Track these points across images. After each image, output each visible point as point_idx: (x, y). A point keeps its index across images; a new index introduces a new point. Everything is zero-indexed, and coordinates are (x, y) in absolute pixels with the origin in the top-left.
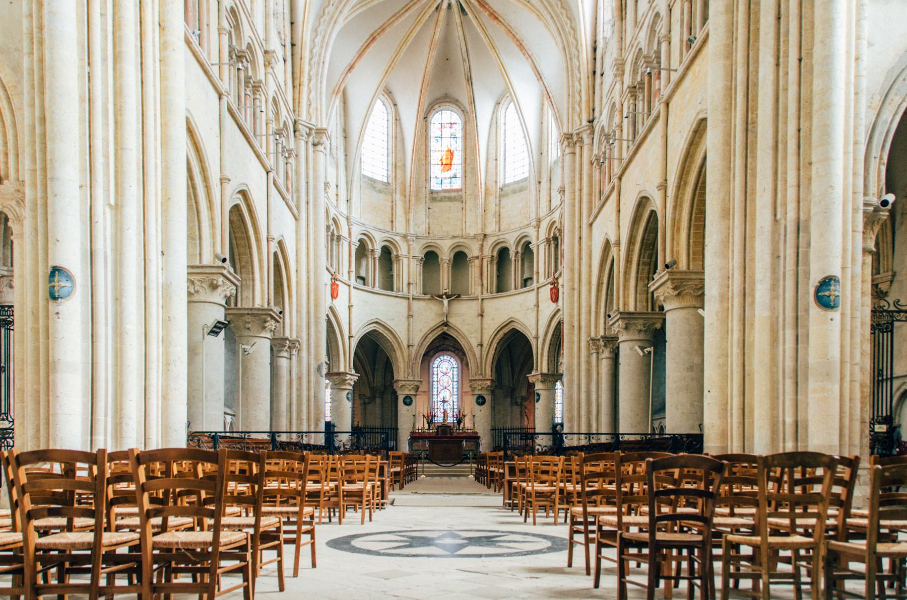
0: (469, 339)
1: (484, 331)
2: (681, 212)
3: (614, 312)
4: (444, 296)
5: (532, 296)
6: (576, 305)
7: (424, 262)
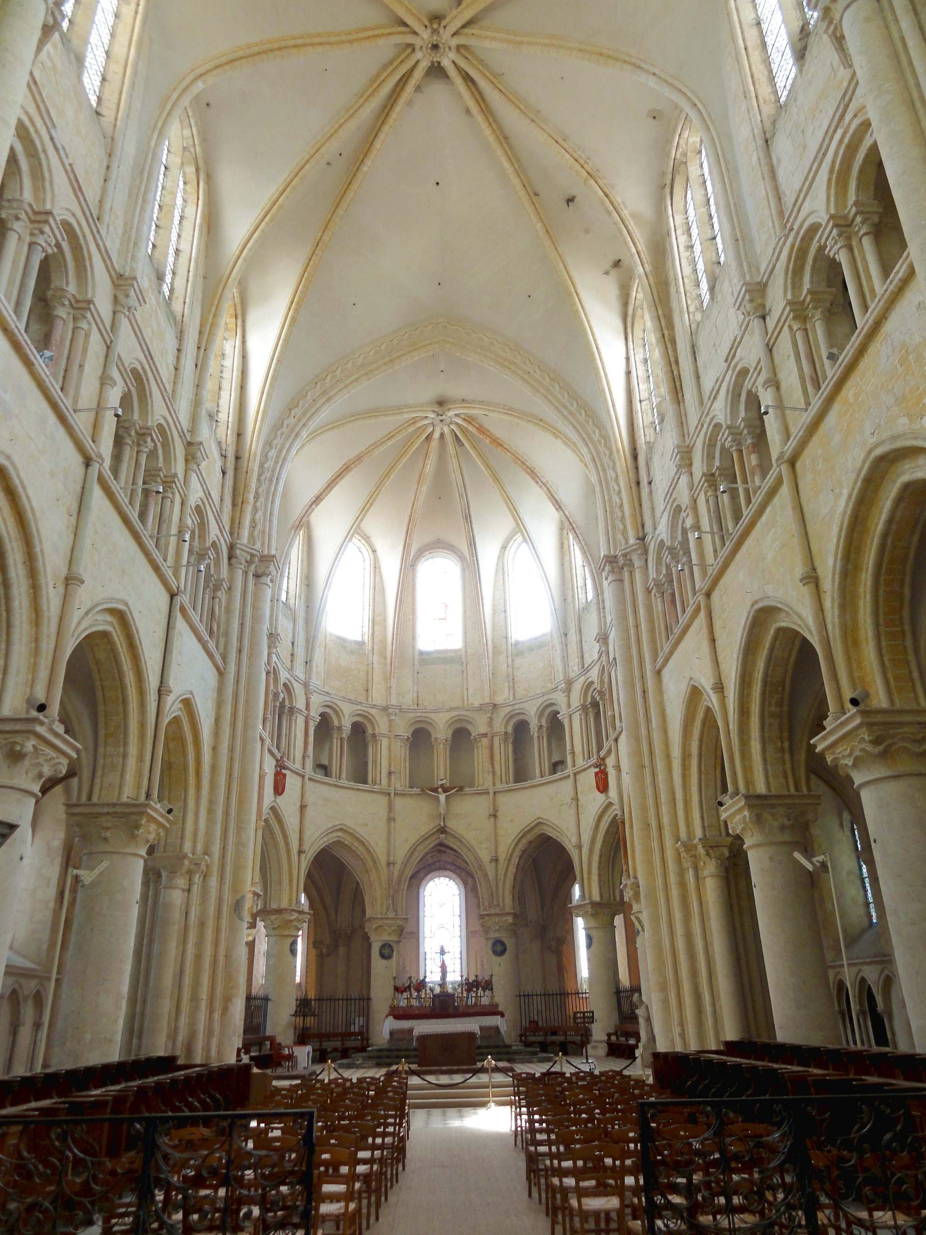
0: (478, 851)
2: (855, 613)
3: (732, 798)
4: (440, 790)
5: (566, 788)
6: (650, 791)
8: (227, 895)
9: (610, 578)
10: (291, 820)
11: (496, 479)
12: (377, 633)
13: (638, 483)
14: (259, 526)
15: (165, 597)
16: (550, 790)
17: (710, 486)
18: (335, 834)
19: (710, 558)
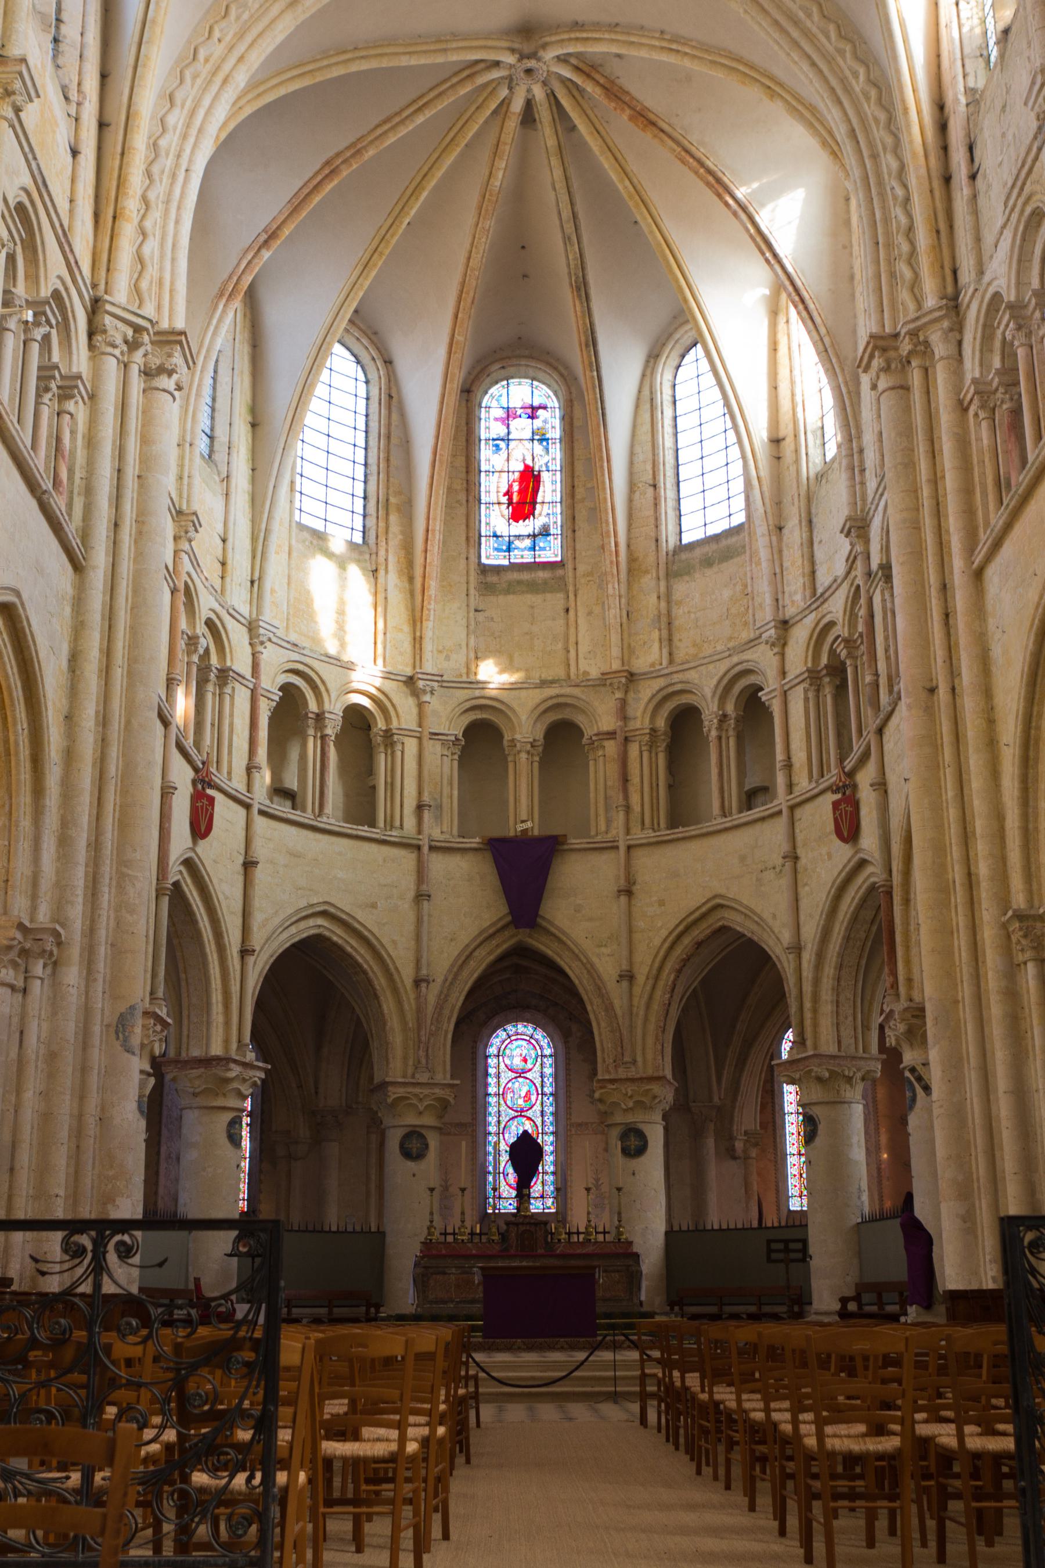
0: (595, 960)
1: (637, 936)
5: (775, 834)
6: (952, 813)
7: (464, 749)
9: (882, 385)
13: (947, 179)
14: (152, 272)
16: (738, 840)
18: (311, 922)
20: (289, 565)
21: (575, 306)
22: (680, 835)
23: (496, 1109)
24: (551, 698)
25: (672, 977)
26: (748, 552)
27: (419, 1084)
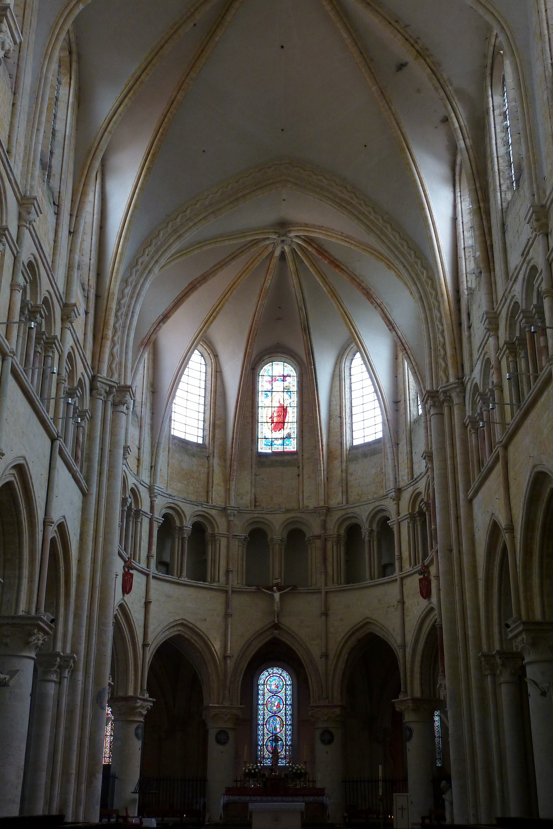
3: (515, 622)
5: (394, 589)
6: (458, 607)
8: (91, 687)
9: (432, 412)
10: (137, 616)
11: (335, 295)
12: (217, 436)
13: (460, 324)
14: (117, 359)
15: (48, 442)
17: (511, 353)
18: (175, 629)
19: (508, 419)
20: (168, 457)
21: (303, 337)
22: (350, 587)
23: (262, 712)
24: (291, 518)
25: (347, 655)
26: (383, 453)
27: (225, 707)
